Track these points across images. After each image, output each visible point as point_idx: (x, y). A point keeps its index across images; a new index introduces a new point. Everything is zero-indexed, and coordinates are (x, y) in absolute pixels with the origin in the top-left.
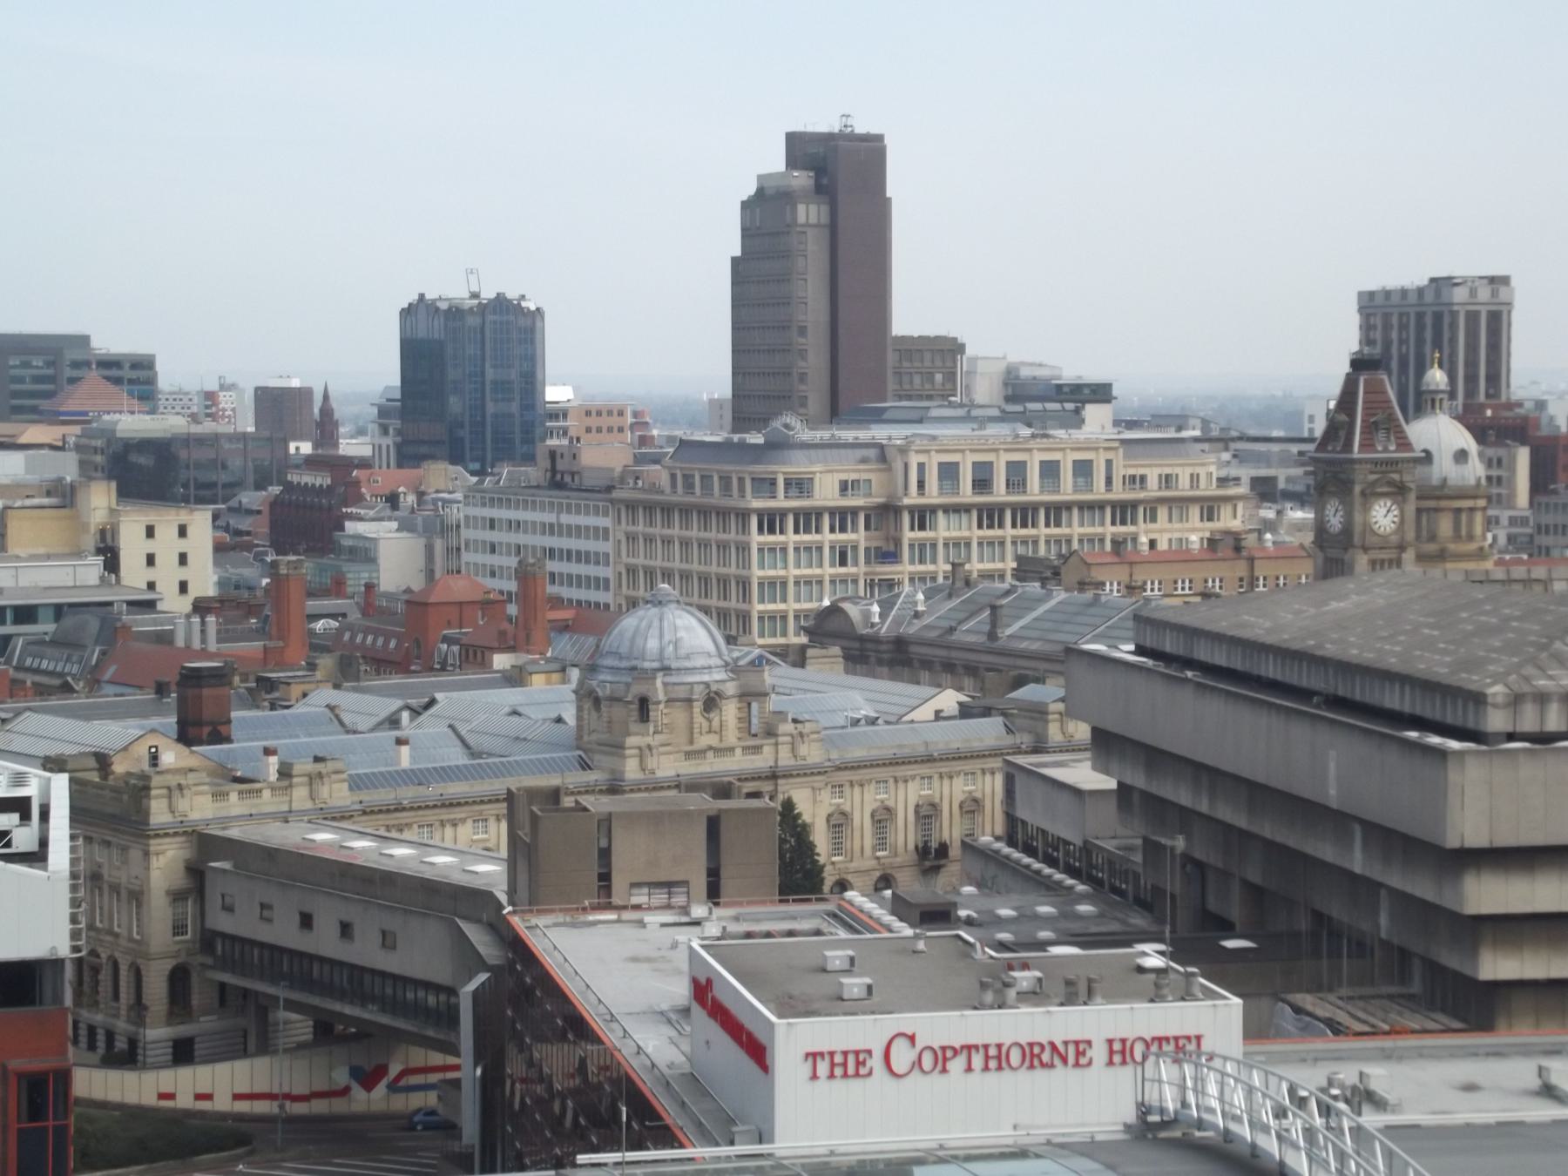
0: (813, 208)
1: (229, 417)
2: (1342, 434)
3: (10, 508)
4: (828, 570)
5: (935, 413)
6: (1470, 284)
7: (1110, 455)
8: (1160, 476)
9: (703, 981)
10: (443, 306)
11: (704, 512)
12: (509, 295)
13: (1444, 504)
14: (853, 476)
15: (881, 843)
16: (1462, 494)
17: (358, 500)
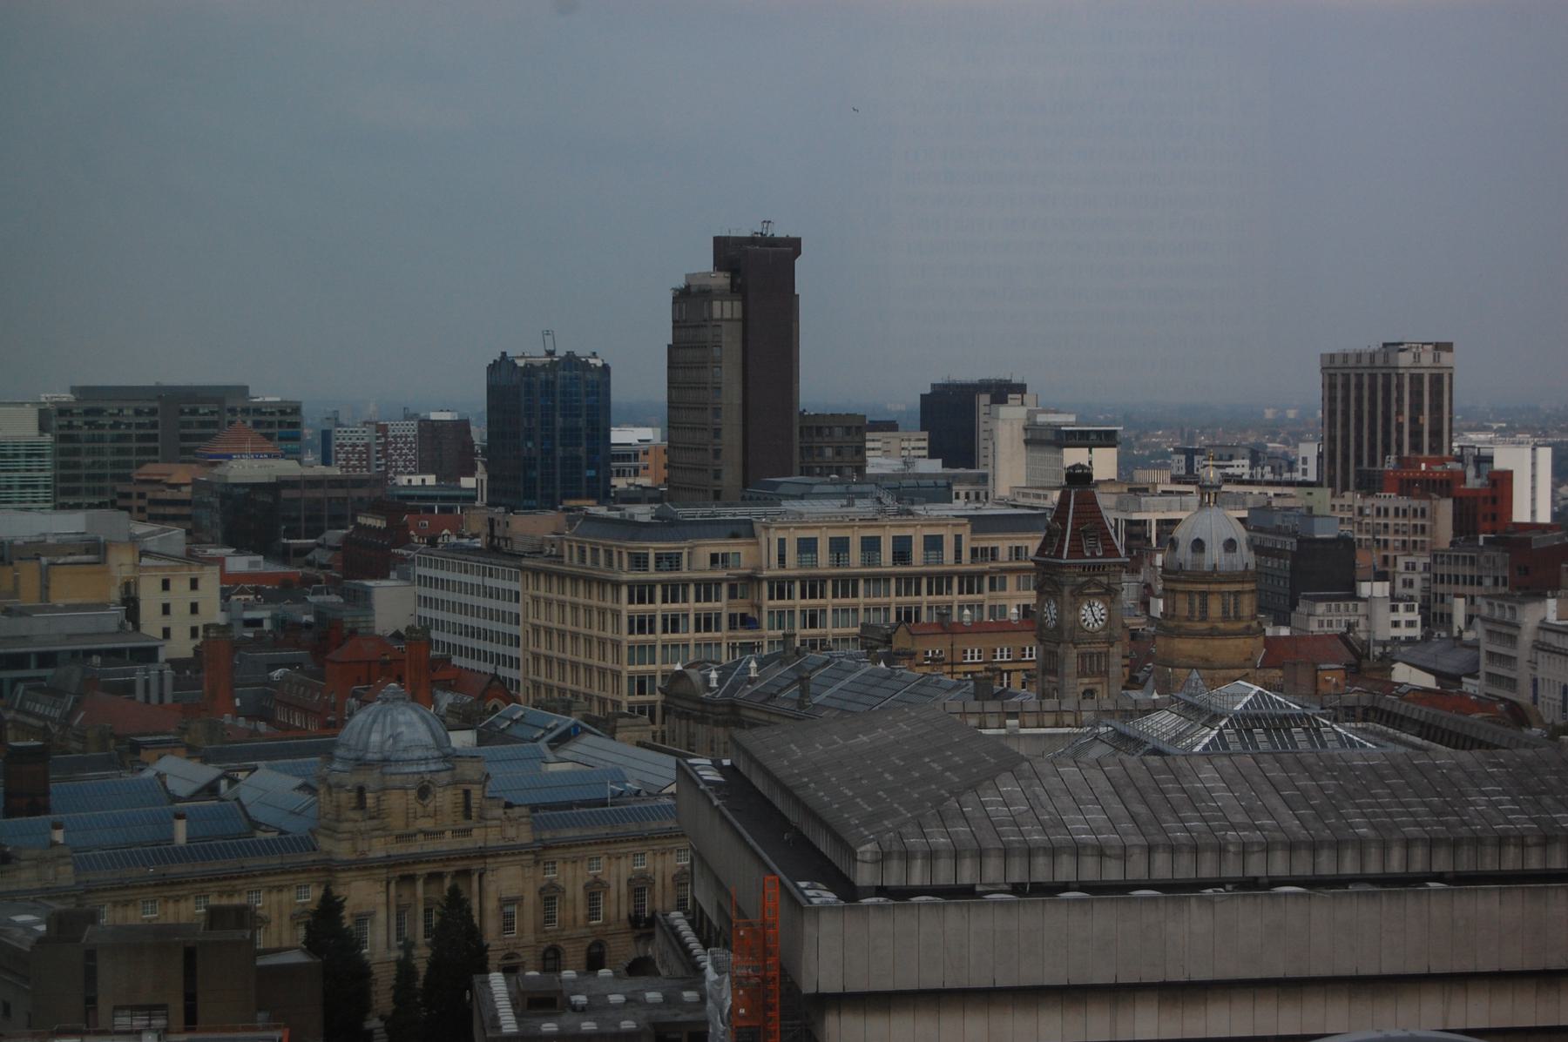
0: (727, 304)
1: (360, 452)
2: (1056, 541)
3: (54, 564)
4: (690, 635)
5: (816, 489)
6: (1414, 350)
7: (959, 531)
8: (1011, 548)
10: (521, 363)
11: (589, 580)
12: (578, 354)
13: (1214, 587)
14: (723, 550)
15: (593, 913)
16: (1231, 578)
17: (406, 541)
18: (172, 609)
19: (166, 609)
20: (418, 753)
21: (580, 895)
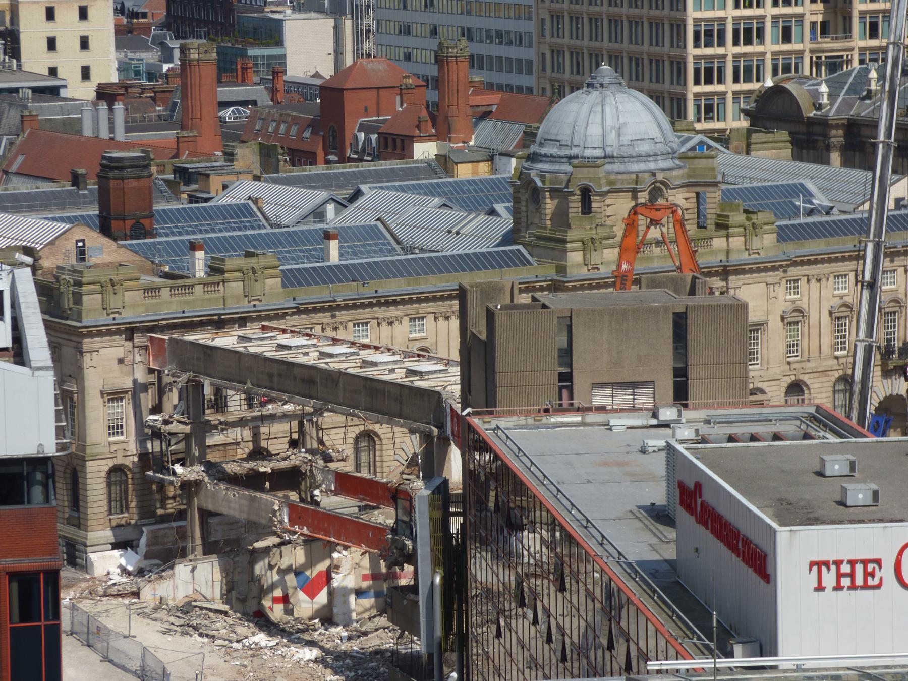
9: (691, 485)
18: (59, 44)
19: (52, 44)
20: (644, 148)
21: (826, 319)
